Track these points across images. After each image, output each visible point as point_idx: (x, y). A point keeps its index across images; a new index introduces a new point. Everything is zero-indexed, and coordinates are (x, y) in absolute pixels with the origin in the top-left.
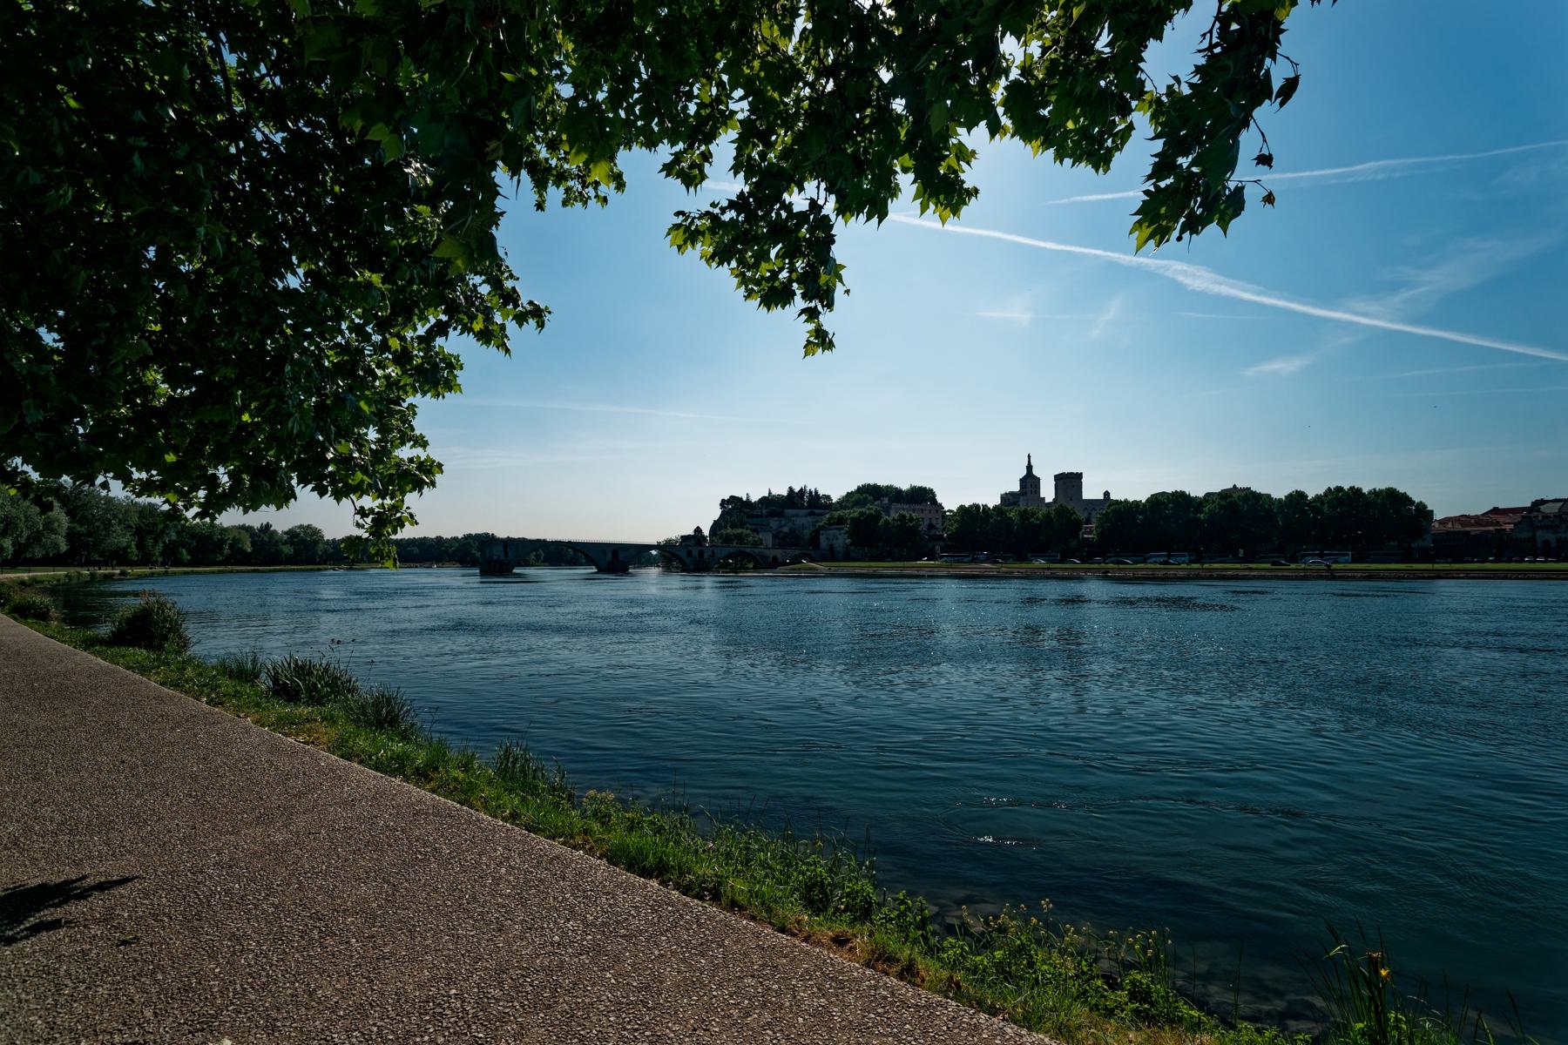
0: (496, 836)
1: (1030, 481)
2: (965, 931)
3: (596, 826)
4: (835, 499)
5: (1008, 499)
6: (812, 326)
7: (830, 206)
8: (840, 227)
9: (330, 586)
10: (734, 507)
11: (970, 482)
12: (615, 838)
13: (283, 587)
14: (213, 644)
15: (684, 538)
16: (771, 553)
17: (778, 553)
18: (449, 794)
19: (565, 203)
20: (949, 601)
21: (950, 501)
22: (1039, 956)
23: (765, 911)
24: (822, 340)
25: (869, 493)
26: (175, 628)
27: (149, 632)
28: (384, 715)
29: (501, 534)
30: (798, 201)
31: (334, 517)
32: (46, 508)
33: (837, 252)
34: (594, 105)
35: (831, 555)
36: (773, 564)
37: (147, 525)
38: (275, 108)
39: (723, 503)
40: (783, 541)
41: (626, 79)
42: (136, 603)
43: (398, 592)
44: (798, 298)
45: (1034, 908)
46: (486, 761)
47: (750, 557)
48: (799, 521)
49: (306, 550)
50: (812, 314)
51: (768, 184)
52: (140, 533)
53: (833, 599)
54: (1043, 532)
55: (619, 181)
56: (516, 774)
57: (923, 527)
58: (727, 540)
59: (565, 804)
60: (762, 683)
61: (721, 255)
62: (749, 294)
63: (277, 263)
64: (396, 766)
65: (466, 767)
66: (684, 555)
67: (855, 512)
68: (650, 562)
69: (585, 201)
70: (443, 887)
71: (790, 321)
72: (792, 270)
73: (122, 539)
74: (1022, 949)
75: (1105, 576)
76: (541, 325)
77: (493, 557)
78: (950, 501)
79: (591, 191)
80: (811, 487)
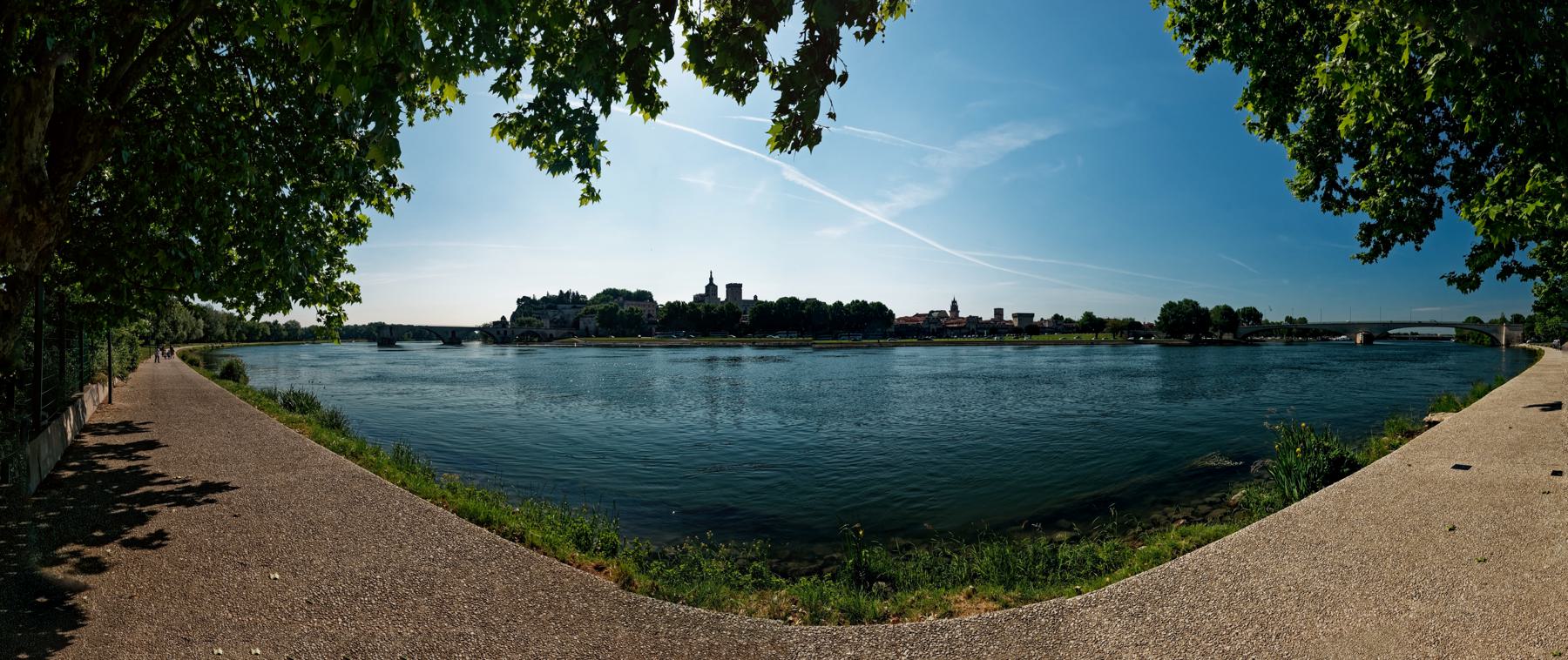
0: (393, 494)
1: (711, 288)
2: (664, 556)
3: (449, 494)
4: (589, 298)
5: (698, 298)
6: (584, 186)
7: (596, 108)
8: (601, 120)
9: (305, 352)
10: (525, 304)
11: (675, 286)
12: (461, 502)
13: (284, 352)
14: (258, 380)
15: (495, 323)
16: (548, 332)
17: (553, 332)
18: (369, 468)
19: (425, 118)
20: (663, 364)
21: (661, 299)
22: (704, 564)
23: (552, 550)
24: (591, 195)
25: (611, 294)
26: (242, 372)
27: (232, 373)
28: (334, 422)
29: (388, 323)
30: (575, 101)
31: (305, 315)
32: (197, 317)
33: (600, 135)
34: (444, 50)
35: (586, 333)
36: (550, 339)
37: (231, 323)
38: (274, 100)
39: (519, 301)
40: (556, 324)
41: (464, 30)
42: (227, 360)
43: (340, 356)
44: (575, 166)
45: (703, 538)
46: (386, 455)
47: (536, 335)
48: (567, 312)
49: (293, 335)
50: (584, 177)
51: (552, 91)
52: (228, 327)
53: (588, 360)
54: (719, 319)
55: (461, 97)
56: (403, 460)
57: (645, 316)
58: (522, 324)
59: (431, 480)
60: (545, 412)
61: (524, 141)
62: (541, 164)
63: (277, 182)
64: (341, 450)
65: (376, 454)
66: (495, 334)
67: (602, 306)
68: (475, 338)
69: (437, 114)
70: (370, 518)
71: (569, 182)
72: (571, 148)
73: (221, 330)
74: (696, 561)
75: (754, 345)
76: (409, 197)
77: (385, 336)
78: (661, 299)
79: (441, 107)
80: (574, 290)
